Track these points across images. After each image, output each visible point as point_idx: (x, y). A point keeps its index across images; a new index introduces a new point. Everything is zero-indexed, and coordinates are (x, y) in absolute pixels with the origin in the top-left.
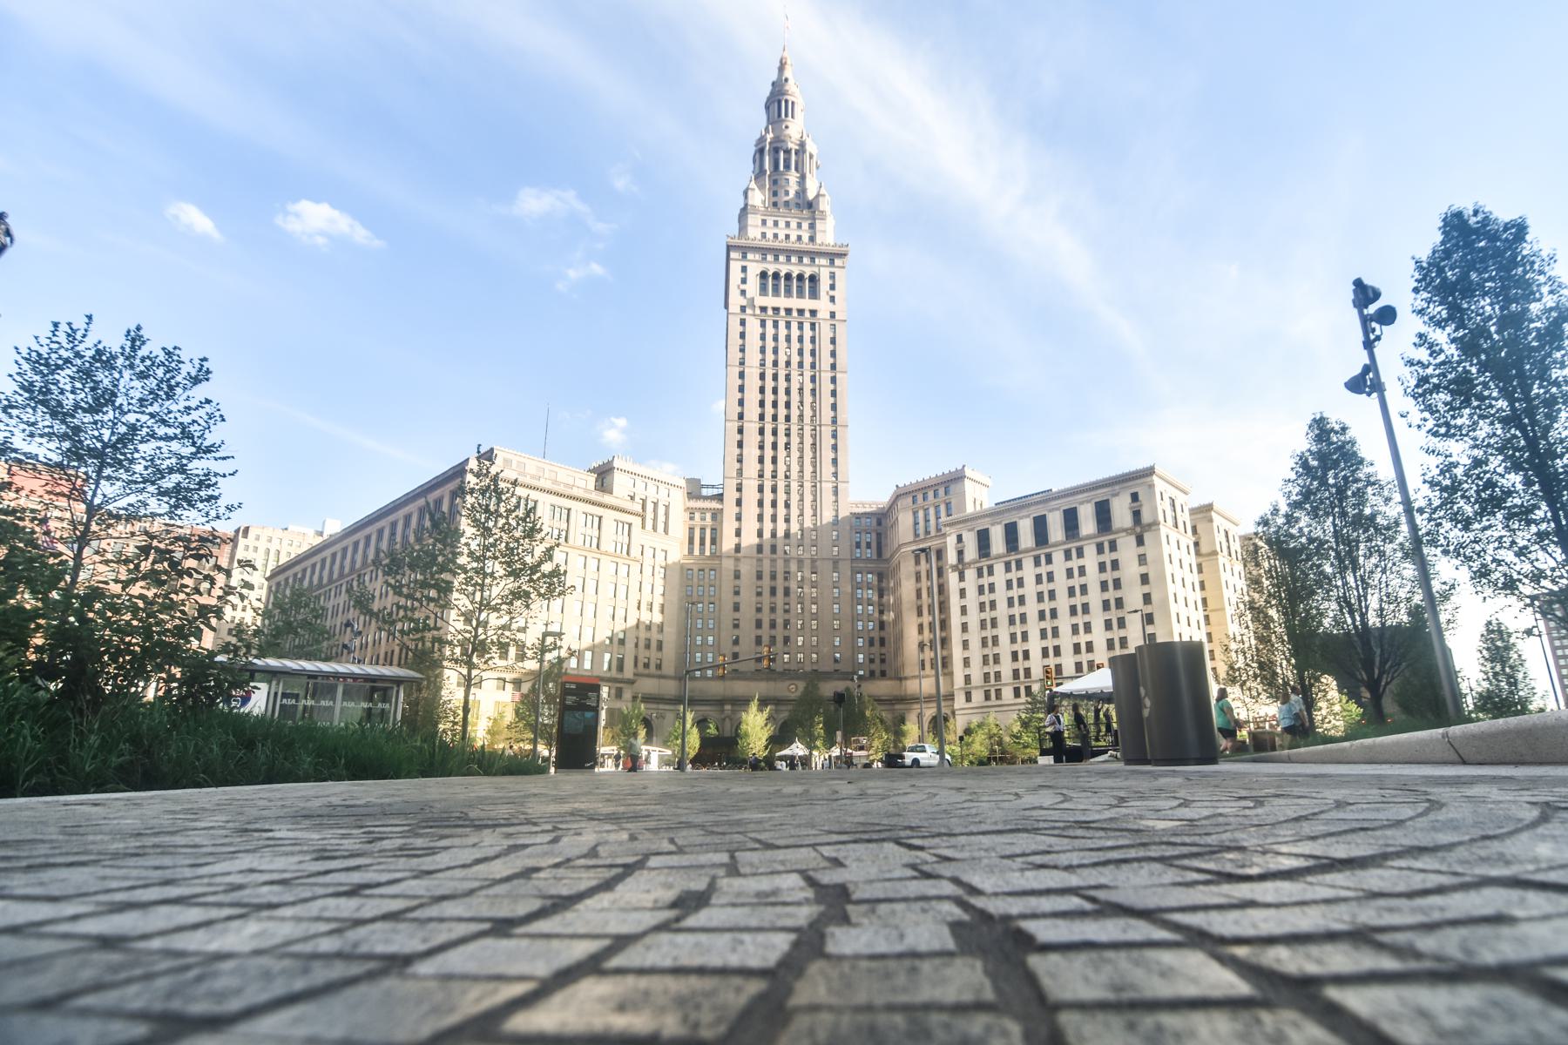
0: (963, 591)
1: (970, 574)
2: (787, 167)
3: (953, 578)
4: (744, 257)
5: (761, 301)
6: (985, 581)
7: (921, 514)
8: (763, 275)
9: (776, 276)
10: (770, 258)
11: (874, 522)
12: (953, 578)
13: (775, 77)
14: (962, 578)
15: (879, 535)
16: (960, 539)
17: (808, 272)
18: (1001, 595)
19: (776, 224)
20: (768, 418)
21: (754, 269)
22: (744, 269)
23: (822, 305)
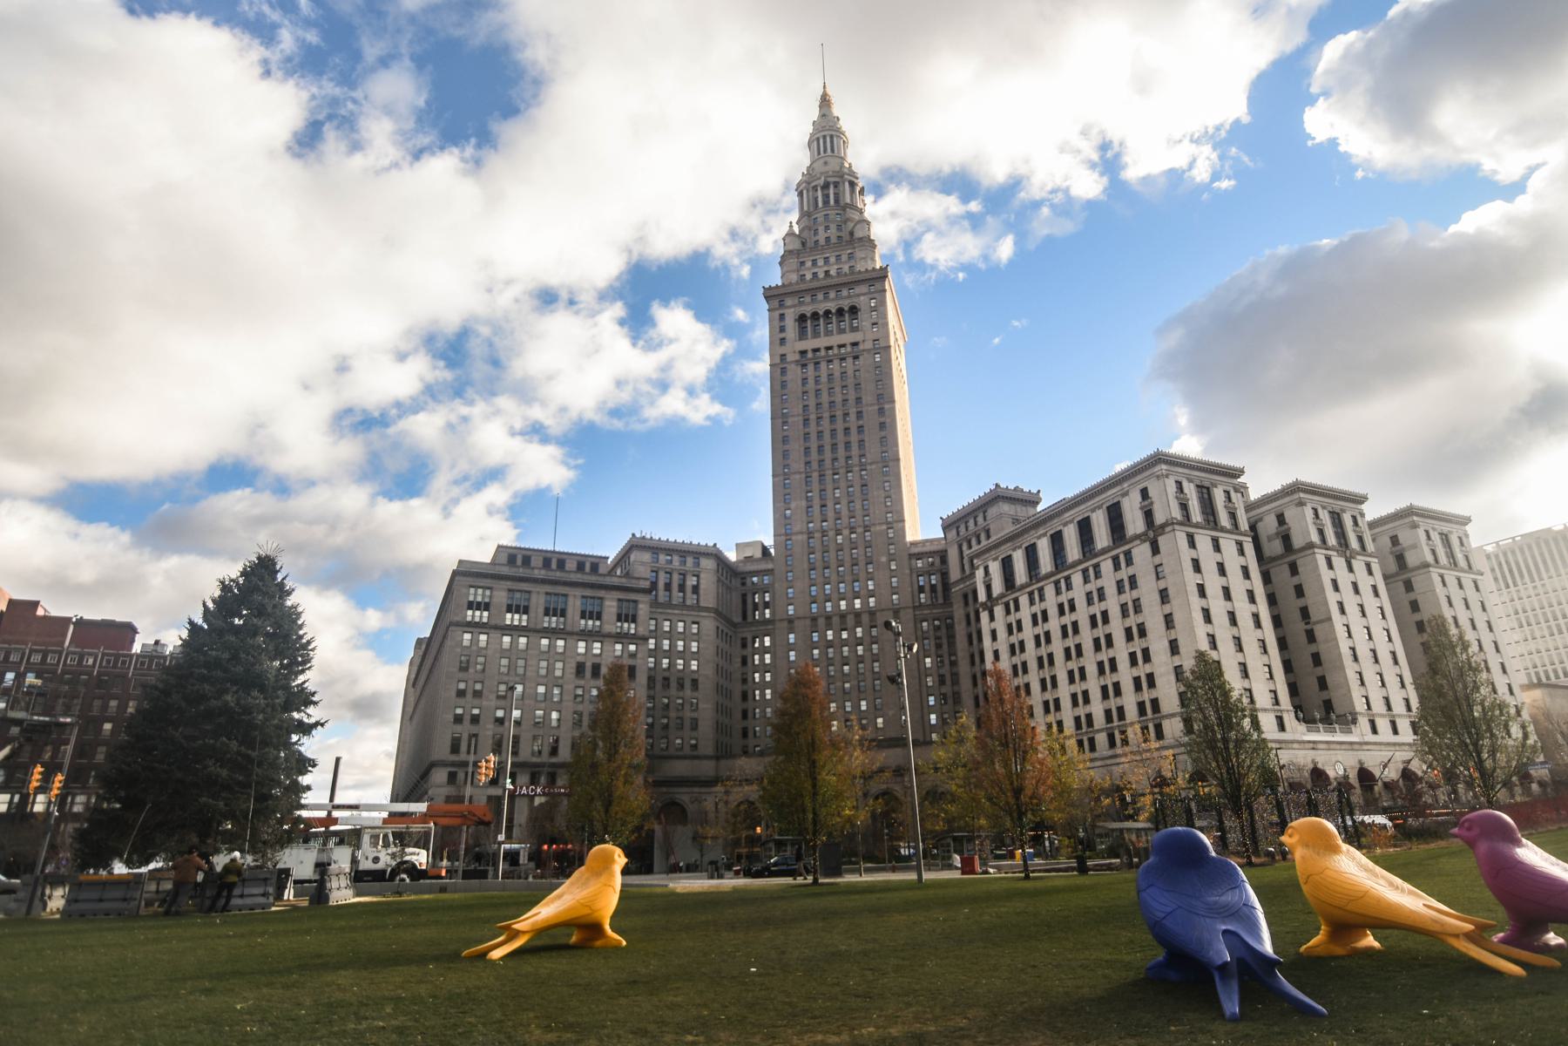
1: (999, 611)
2: (826, 202)
4: (781, 305)
6: (1012, 619)
7: (965, 547)
8: (802, 319)
9: (815, 316)
10: (808, 299)
14: (992, 618)
17: (846, 304)
19: (814, 262)
20: (815, 465)
21: (790, 316)
22: (782, 316)
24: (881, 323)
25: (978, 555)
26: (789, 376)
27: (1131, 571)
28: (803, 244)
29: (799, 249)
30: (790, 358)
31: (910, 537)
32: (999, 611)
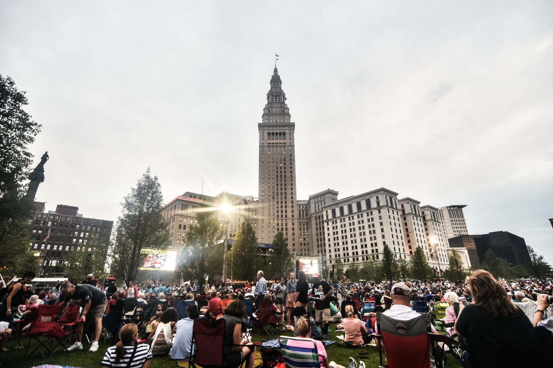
0: (328, 228)
1: (330, 223)
3: (325, 224)
5: (269, 141)
6: (335, 225)
7: (317, 204)
8: (269, 134)
9: (273, 133)
11: (305, 207)
12: (325, 224)
13: (273, 74)
14: (328, 224)
15: (306, 211)
16: (327, 212)
18: (339, 230)
21: (266, 132)
23: (287, 141)
24: (292, 138)
25: (325, 207)
26: (265, 150)
27: (372, 216)
28: (269, 112)
29: (268, 113)
30: (266, 144)
31: (298, 199)
32: (330, 223)
